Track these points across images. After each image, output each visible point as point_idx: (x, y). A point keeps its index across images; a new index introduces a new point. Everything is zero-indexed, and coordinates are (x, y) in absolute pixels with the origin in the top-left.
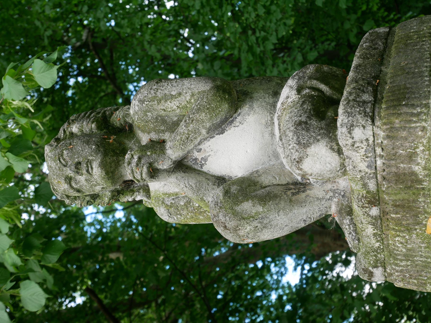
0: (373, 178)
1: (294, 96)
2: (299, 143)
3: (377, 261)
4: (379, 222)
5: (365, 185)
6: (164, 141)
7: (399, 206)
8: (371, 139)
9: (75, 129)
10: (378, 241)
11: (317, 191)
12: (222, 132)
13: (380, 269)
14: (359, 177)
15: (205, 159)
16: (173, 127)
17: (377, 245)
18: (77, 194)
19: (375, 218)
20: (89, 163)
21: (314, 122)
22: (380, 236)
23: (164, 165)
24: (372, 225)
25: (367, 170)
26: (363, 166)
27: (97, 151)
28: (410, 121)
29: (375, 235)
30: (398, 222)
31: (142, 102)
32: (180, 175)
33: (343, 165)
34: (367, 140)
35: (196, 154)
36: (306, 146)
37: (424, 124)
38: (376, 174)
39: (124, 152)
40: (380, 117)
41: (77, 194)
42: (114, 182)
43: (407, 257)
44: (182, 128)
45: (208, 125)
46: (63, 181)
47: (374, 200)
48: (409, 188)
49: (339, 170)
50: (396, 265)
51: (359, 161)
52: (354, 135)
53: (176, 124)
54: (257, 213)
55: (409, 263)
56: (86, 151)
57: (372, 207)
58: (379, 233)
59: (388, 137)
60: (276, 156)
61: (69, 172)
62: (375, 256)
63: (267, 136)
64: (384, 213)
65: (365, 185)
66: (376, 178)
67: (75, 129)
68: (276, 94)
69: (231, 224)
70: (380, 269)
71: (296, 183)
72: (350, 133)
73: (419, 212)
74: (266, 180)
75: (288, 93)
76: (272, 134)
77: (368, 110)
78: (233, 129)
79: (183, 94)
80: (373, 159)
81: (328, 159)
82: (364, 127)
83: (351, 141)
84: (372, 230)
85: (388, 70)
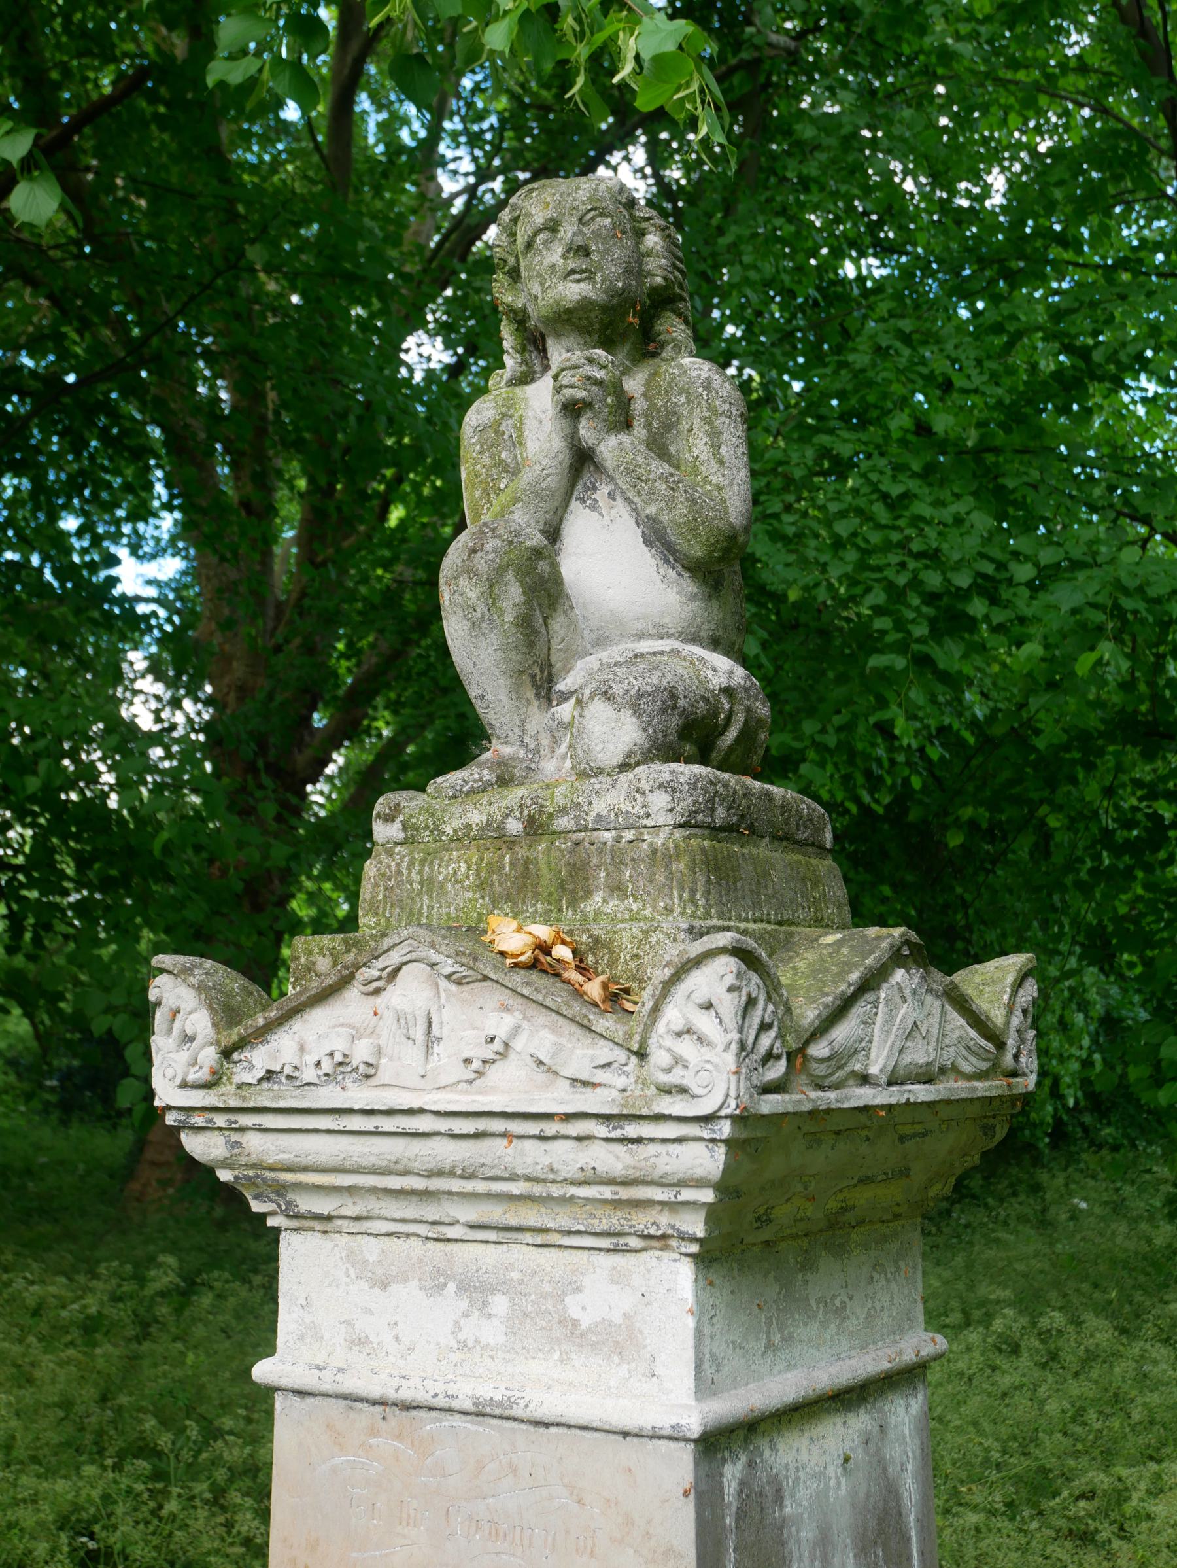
1: (717, 681)
2: (640, 696)
4: (494, 834)
5: (564, 810)
6: (628, 425)
7: (526, 869)
8: (649, 822)
9: (653, 240)
11: (537, 719)
12: (647, 542)
13: (402, 835)
15: (594, 507)
16: (658, 446)
17: (449, 830)
18: (521, 240)
19: (501, 827)
20: (589, 275)
21: (675, 722)
22: (464, 836)
23: (587, 430)
26: (600, 807)
27: (612, 292)
28: (682, 889)
29: (468, 826)
30: (495, 867)
31: (707, 385)
32: (566, 458)
33: (599, 772)
34: (648, 816)
35: (604, 490)
36: (636, 709)
37: (678, 910)
38: (586, 829)
39: (608, 344)
40: (688, 837)
41: (521, 240)
42: (547, 320)
43: (428, 883)
44: (658, 468)
45: (664, 518)
46: (549, 214)
47: (536, 826)
48: (561, 886)
50: (411, 864)
51: (610, 799)
52: (657, 793)
53: (662, 453)
54: (501, 612)
55: (416, 886)
56: (611, 270)
59: (654, 851)
60: (601, 642)
61: (568, 231)
63: (639, 626)
64: (512, 843)
65: (564, 810)
67: (653, 240)
68: (715, 644)
69: (481, 563)
70: (402, 835)
71: (550, 680)
72: (661, 786)
73: (515, 904)
74: (558, 625)
75: (722, 670)
76: (641, 636)
77: (700, 817)
78: (654, 562)
79: (719, 470)
81: (611, 747)
82: (671, 810)
83: (647, 787)
85: (762, 850)
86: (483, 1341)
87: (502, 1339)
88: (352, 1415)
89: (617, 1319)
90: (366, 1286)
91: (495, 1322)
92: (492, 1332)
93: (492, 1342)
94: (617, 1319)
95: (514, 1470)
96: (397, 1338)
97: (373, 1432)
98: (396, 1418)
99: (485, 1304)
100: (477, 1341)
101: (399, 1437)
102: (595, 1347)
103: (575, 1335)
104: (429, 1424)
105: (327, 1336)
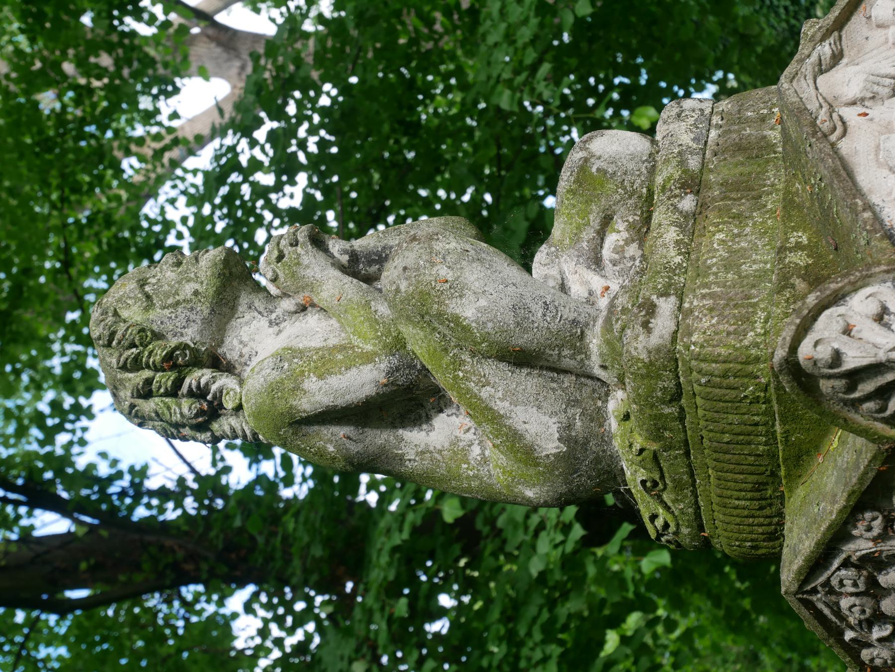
0: (697, 154)
3: (670, 285)
5: (682, 163)
10: (679, 254)
13: (673, 299)
14: (676, 151)
17: (678, 259)
19: (686, 216)
22: (686, 248)
24: (676, 226)
25: (691, 144)
26: (686, 139)
29: (678, 243)
43: (728, 265)
47: (692, 183)
49: (646, 160)
57: (686, 194)
58: (686, 240)
62: (669, 277)
64: (702, 207)
66: (704, 154)
70: (673, 299)
80: (704, 131)
84: (675, 235)
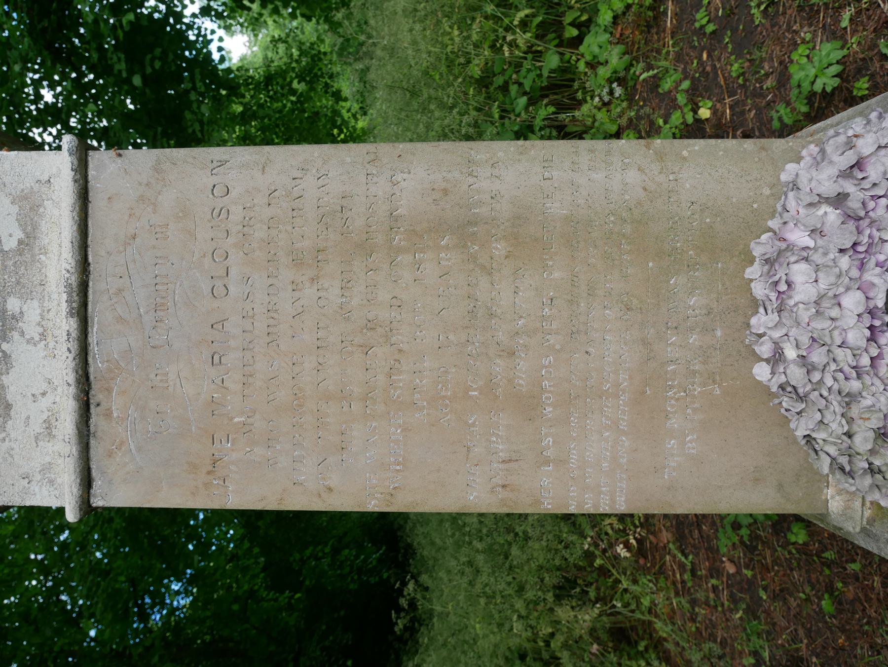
86: (38, 319)
87: (36, 303)
88: (99, 434)
89: (15, 209)
90: (10, 422)
91: (25, 308)
92: (32, 312)
93: (38, 311)
94: (15, 209)
95: (120, 291)
96: (44, 394)
97: (108, 414)
98: (96, 395)
99: (14, 317)
100: (39, 324)
101: (109, 390)
102: (35, 227)
103: (28, 242)
104: (97, 365)
105: (48, 459)
